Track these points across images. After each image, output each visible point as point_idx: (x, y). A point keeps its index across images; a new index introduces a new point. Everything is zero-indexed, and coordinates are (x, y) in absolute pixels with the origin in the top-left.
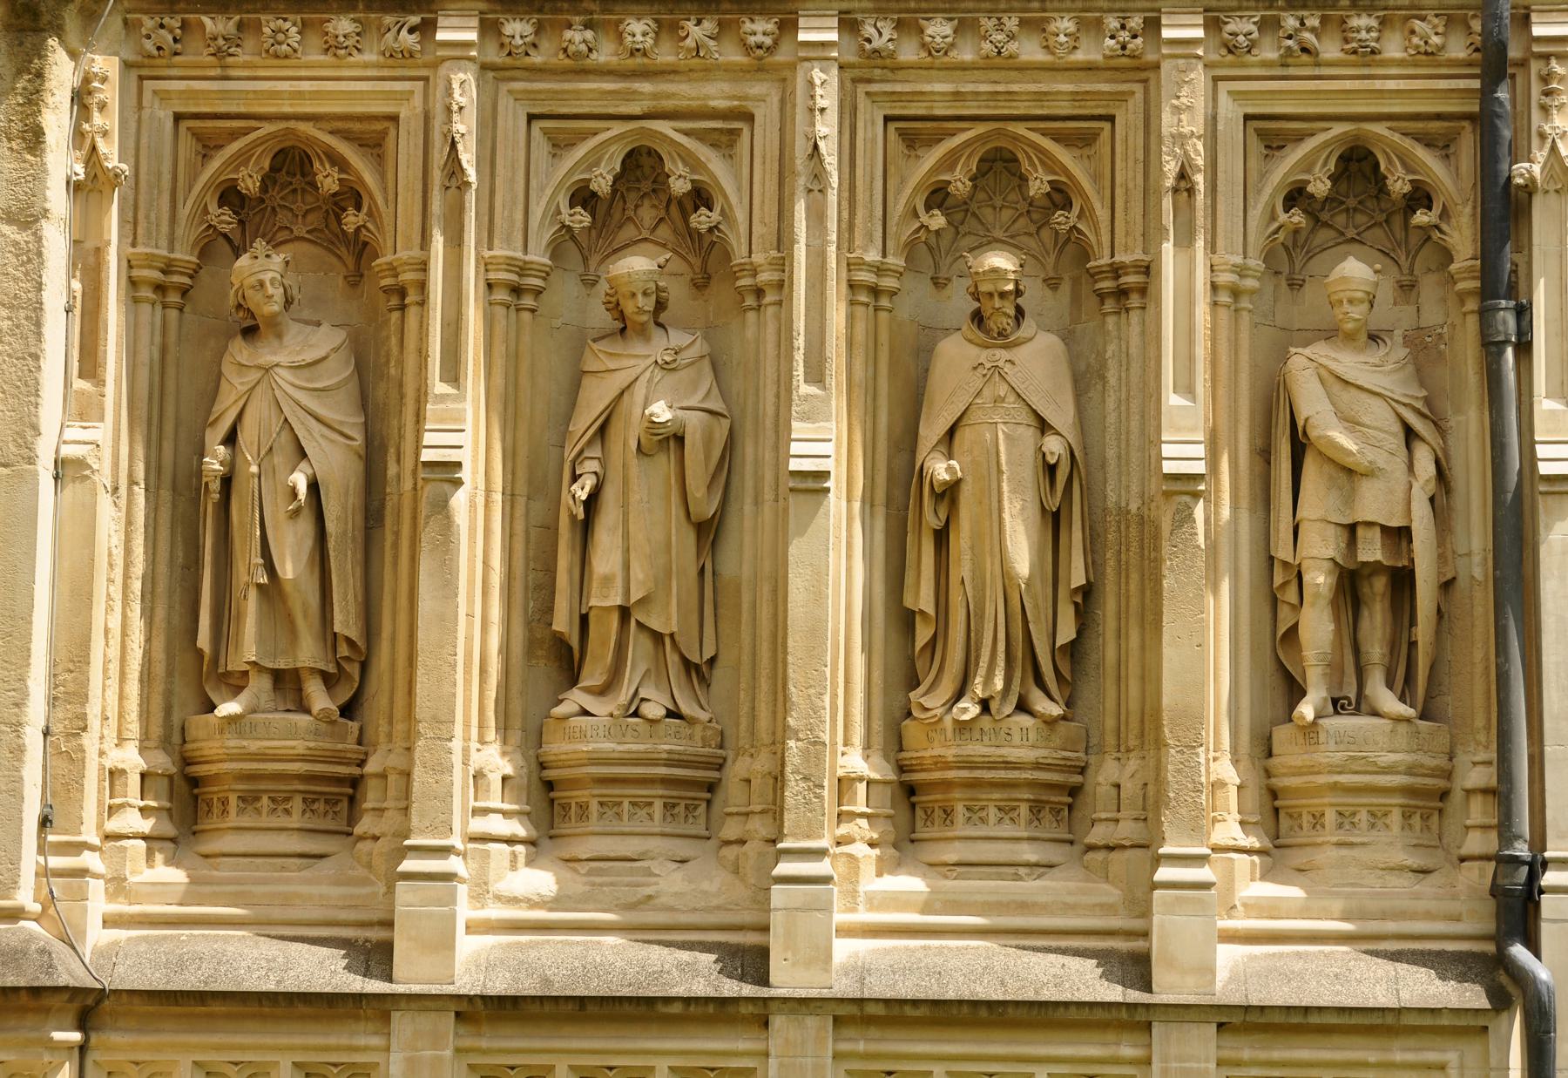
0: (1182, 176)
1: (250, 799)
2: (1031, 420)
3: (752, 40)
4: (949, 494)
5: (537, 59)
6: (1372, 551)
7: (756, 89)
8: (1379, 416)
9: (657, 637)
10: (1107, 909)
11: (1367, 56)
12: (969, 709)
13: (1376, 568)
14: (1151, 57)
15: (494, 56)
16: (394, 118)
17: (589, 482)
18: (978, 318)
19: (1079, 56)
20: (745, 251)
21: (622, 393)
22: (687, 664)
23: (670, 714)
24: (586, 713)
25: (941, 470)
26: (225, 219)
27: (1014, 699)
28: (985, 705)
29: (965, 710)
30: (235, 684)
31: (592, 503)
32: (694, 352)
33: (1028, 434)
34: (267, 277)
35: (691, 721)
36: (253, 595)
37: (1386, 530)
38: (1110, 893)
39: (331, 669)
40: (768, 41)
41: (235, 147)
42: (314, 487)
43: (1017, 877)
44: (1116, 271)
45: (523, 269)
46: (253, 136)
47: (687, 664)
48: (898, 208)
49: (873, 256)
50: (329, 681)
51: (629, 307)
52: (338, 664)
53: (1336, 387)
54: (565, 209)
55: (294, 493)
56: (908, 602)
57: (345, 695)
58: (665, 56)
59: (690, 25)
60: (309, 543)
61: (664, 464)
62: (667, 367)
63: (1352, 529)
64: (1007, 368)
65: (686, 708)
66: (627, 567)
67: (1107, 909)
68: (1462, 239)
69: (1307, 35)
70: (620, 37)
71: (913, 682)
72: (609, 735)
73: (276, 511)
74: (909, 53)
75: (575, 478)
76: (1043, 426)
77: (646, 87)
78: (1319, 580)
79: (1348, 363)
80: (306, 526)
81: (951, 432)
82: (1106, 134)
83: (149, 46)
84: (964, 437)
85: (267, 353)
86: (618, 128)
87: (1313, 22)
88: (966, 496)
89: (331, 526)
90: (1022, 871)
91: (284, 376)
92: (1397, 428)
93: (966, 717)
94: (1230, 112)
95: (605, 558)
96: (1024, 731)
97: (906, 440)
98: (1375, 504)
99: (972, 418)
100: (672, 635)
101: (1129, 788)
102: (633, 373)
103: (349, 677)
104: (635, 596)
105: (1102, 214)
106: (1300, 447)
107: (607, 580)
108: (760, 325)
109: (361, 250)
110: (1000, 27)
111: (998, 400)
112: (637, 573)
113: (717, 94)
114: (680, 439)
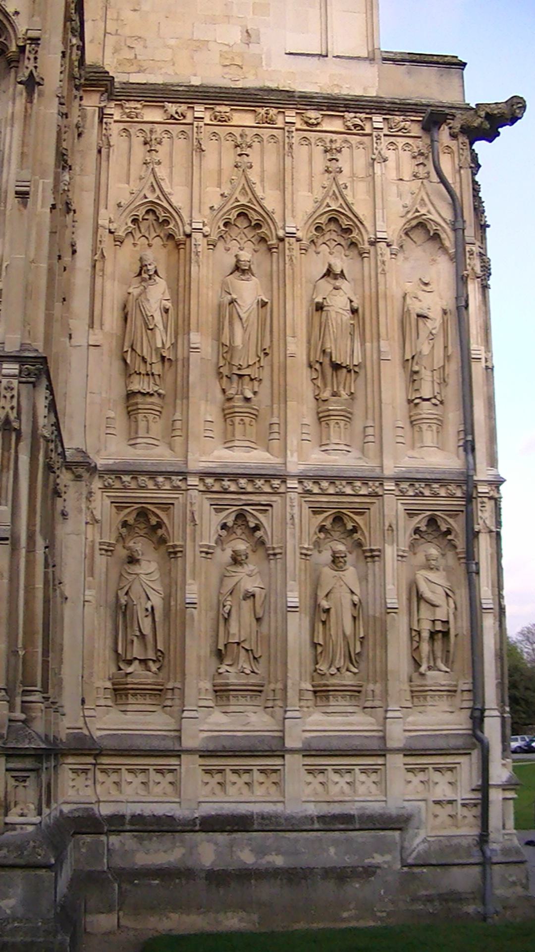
0: (390, 526)
1: (134, 695)
2: (349, 591)
3: (274, 486)
4: (327, 611)
5: (214, 489)
6: (439, 627)
7: (274, 498)
8: (440, 591)
9: (247, 650)
10: (372, 724)
11: (436, 495)
12: (333, 670)
13: (439, 631)
14: (381, 493)
15: (202, 488)
16: (173, 504)
17: (228, 607)
18: (333, 562)
19: (361, 493)
20: (270, 543)
21: (237, 584)
22: (255, 658)
23: (253, 672)
24: (228, 671)
25: (325, 604)
26: (124, 531)
27: (345, 668)
28: (338, 669)
29: (333, 671)
30: (129, 662)
31: (229, 614)
32: (255, 571)
33: (349, 595)
34: (138, 549)
35: (257, 674)
36: (135, 639)
37: (443, 622)
38: (372, 720)
39: (155, 659)
40: (278, 486)
41: (128, 510)
42: (152, 608)
43: (347, 716)
44: (372, 551)
45: (209, 547)
46: (133, 508)
47: (255, 658)
48: (312, 531)
49: (306, 546)
50: (154, 661)
51: (239, 558)
52: (157, 658)
53: (430, 583)
54: (220, 531)
55: (147, 610)
56: (316, 641)
57: (158, 665)
58: (250, 489)
59: (257, 481)
60: (151, 623)
61: (249, 602)
62: (250, 576)
63: (433, 621)
64: (343, 577)
65: (256, 671)
66: (239, 631)
67: (372, 724)
68: (461, 543)
69: (421, 489)
70: (237, 484)
71: (317, 663)
72: (236, 678)
73: (141, 614)
74: (316, 490)
75: (224, 606)
76: (352, 592)
77: (243, 497)
78: (425, 635)
79: (432, 576)
80: (150, 619)
81: (327, 595)
82: (367, 514)
83: (106, 484)
84: (331, 596)
85: (136, 569)
86: (235, 508)
87: (423, 486)
88: (332, 611)
89: (157, 619)
90: (349, 714)
91: (143, 577)
92: (444, 594)
93: (333, 673)
94: (401, 508)
95: (234, 628)
96: (348, 676)
97: (315, 597)
98: (441, 614)
99: (335, 590)
100: (252, 650)
101: (377, 692)
102: (240, 577)
103: (160, 661)
104: (242, 639)
105: (367, 534)
106: (420, 597)
107: (234, 635)
108: (276, 563)
109: (163, 541)
110: (341, 485)
111: (341, 586)
112: (242, 633)
113: (263, 499)
114: (254, 596)
